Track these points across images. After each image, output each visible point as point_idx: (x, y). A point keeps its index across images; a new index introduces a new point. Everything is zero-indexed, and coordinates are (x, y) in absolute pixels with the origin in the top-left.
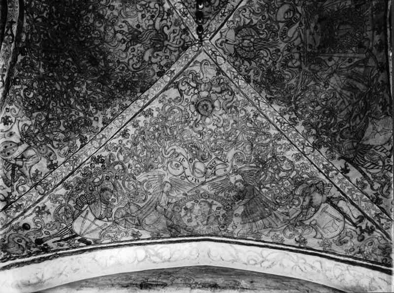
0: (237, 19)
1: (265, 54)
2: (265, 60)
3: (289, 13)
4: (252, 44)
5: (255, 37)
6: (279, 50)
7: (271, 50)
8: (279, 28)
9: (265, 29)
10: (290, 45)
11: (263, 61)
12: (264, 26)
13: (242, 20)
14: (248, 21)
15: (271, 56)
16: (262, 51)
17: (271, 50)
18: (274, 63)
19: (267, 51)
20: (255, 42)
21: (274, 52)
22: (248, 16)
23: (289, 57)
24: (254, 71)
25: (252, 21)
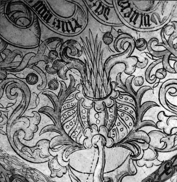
0: (45, 152)
1: (120, 68)
2: (135, 66)
3: (16, 15)
4: (99, 103)
5: (81, 95)
6: (107, 35)
7: (107, 54)
8: (54, 39)
9: (58, 72)
10: (94, 8)
11: (139, 72)
12: (52, 77)
13: (45, 136)
14: (46, 121)
15: (121, 54)
16: (113, 77)
17: (107, 54)
18: (139, 44)
19: (112, 62)
20: (92, 95)
21: (111, 46)
22: (34, 121)
23: (123, 8)
24: (170, 93)
25: (43, 111)
